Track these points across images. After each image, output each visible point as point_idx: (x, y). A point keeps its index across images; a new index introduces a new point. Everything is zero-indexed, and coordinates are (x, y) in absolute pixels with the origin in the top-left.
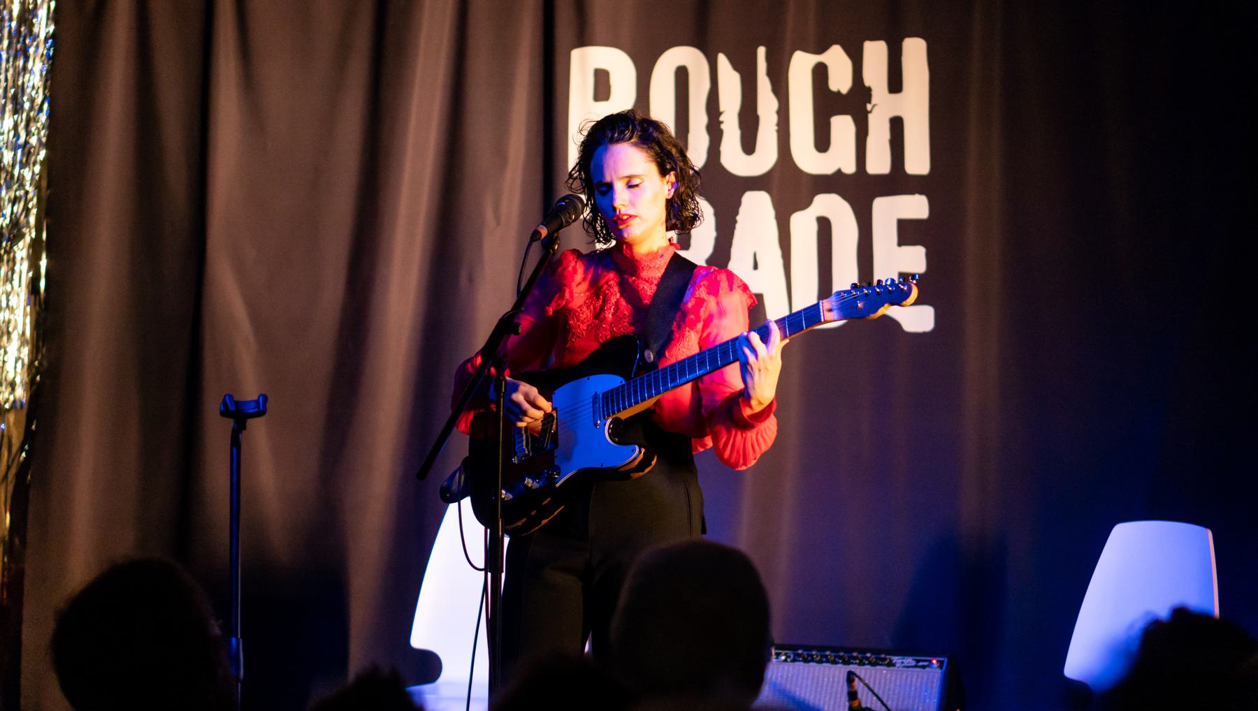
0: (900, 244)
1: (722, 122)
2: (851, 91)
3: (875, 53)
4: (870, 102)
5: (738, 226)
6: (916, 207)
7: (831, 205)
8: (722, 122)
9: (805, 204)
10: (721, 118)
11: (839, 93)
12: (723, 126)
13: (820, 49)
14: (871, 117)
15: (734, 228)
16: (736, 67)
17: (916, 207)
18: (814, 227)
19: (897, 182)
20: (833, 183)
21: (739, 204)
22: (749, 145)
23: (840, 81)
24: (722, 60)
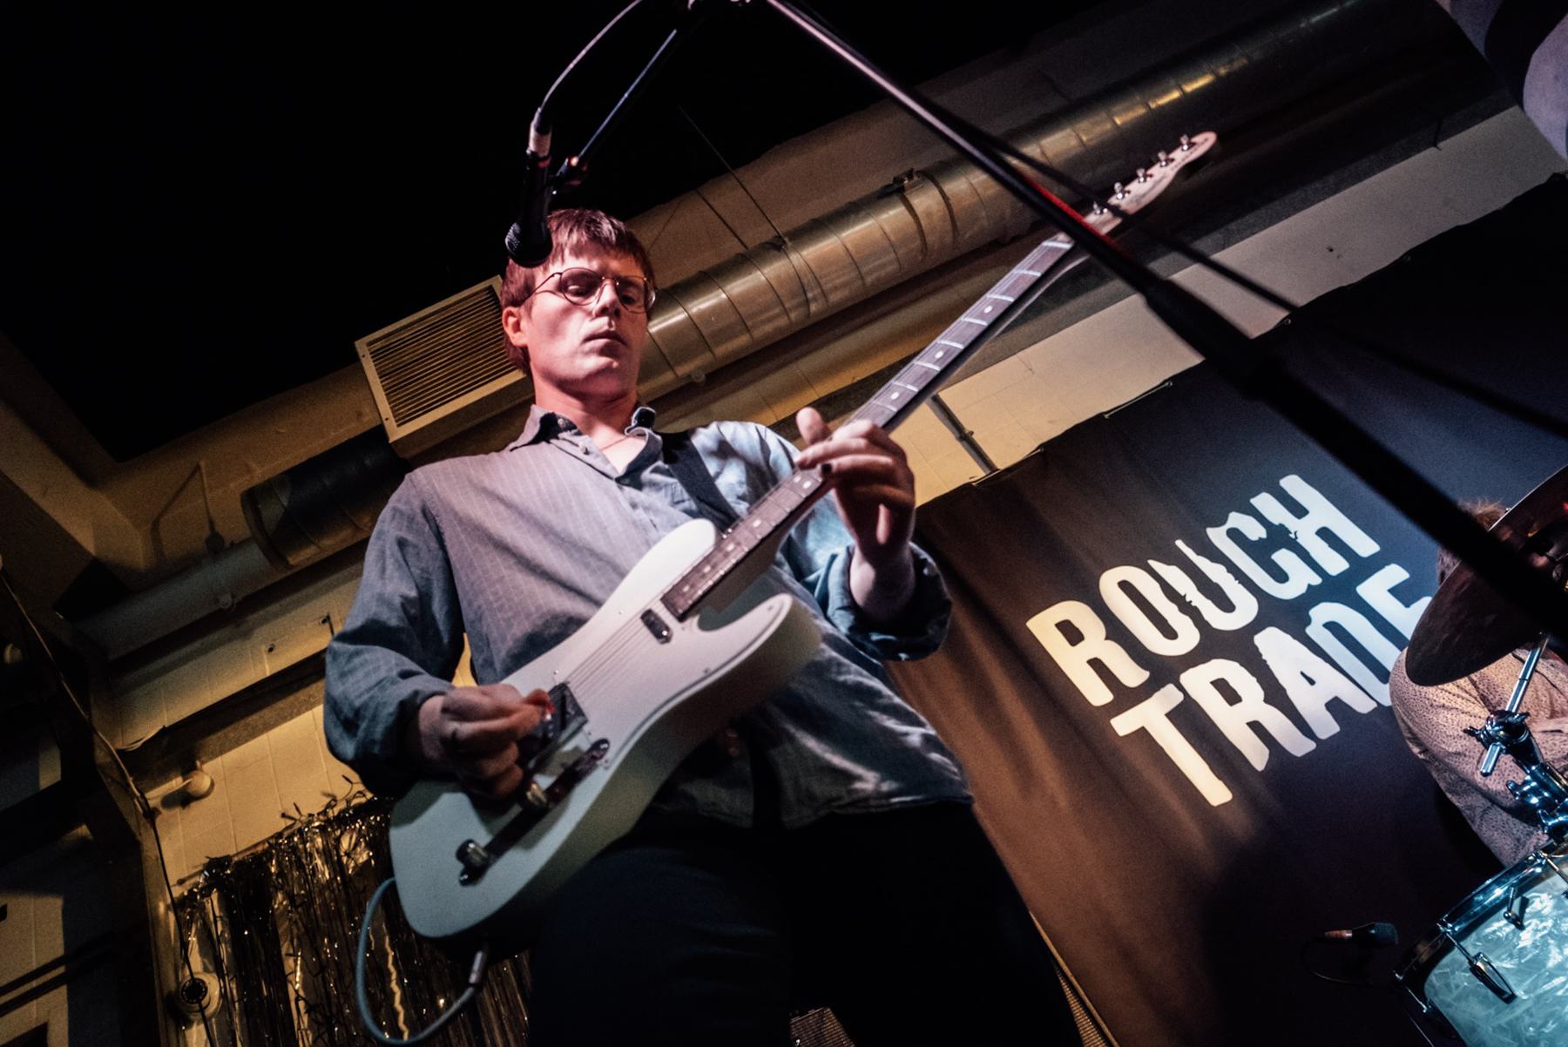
1: (1191, 602)
2: (1268, 533)
5: (1268, 663)
7: (1323, 613)
8: (1191, 602)
9: (1308, 621)
10: (1188, 599)
12: (1193, 604)
13: (1223, 522)
14: (1298, 540)
15: (1268, 667)
16: (1168, 561)
17: (1395, 574)
19: (1362, 568)
20: (1313, 596)
21: (1257, 648)
22: (1226, 605)
23: (1255, 531)
24: (1153, 563)
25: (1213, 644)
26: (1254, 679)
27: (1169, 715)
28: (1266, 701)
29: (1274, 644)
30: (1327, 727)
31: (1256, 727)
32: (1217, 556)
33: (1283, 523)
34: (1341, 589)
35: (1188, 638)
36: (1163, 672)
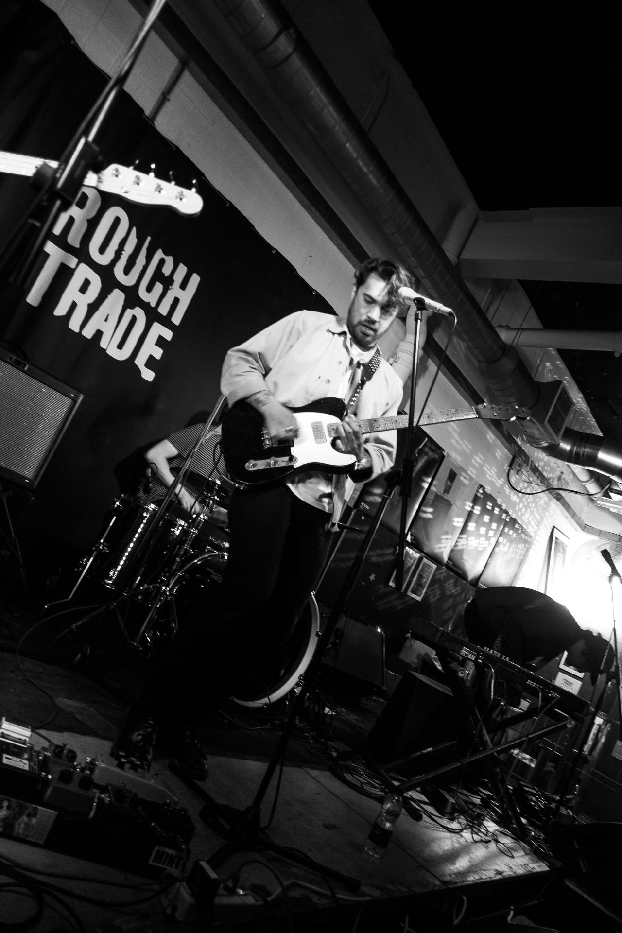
0: (156, 344)
1: (122, 254)
2: (168, 277)
4: (171, 286)
6: (168, 335)
7: (139, 313)
9: (132, 308)
10: (123, 252)
11: (164, 274)
12: (122, 256)
16: (138, 236)
17: (168, 335)
19: (166, 321)
20: (145, 306)
21: (111, 291)
22: (127, 271)
23: (167, 270)
25: (106, 273)
26: (96, 296)
28: (90, 306)
29: (117, 298)
30: (88, 333)
31: (74, 305)
32: (149, 258)
34: (153, 316)
35: (104, 260)
36: (83, 255)
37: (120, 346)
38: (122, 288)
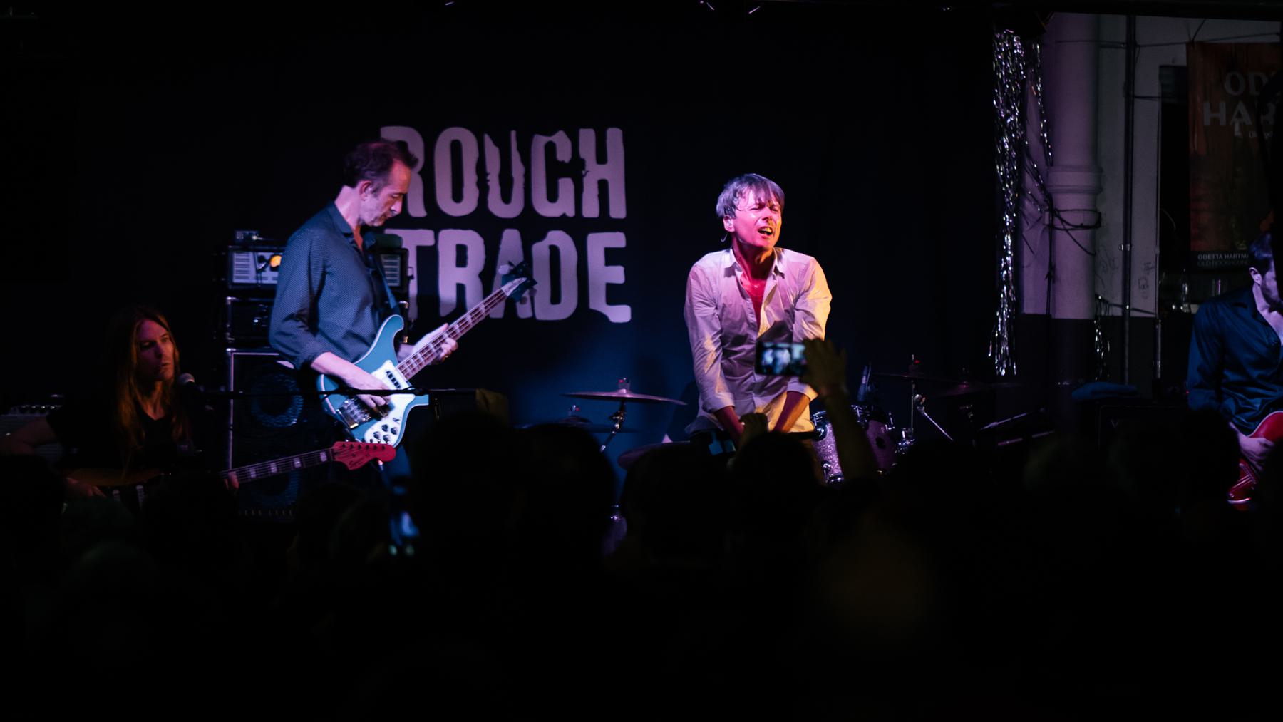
1: (488, 181)
2: (571, 161)
3: (587, 137)
7: (557, 238)
8: (488, 181)
9: (542, 237)
10: (488, 178)
11: (563, 162)
12: (489, 183)
13: (550, 133)
16: (496, 143)
18: (546, 253)
19: (604, 223)
20: (560, 223)
23: (564, 154)
27: (421, 250)
29: (511, 240)
33: (587, 160)
35: (467, 206)
36: (437, 220)
37: (556, 298)
38: (509, 223)
